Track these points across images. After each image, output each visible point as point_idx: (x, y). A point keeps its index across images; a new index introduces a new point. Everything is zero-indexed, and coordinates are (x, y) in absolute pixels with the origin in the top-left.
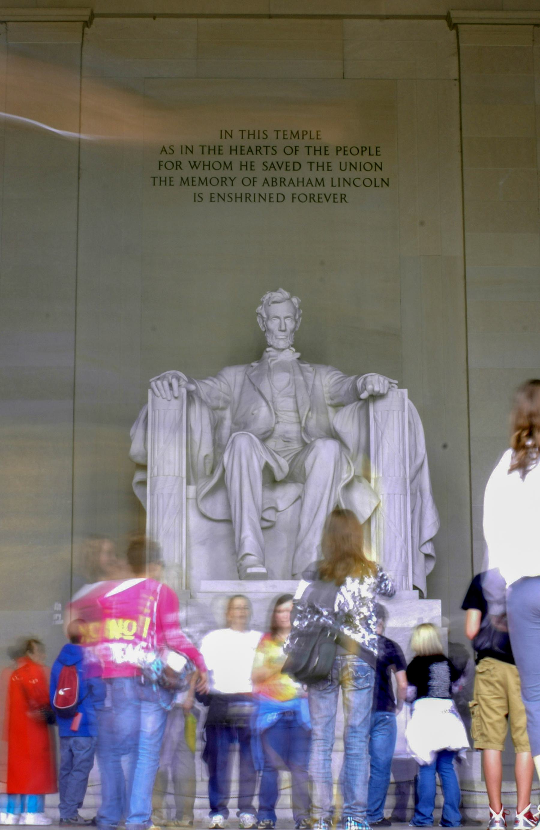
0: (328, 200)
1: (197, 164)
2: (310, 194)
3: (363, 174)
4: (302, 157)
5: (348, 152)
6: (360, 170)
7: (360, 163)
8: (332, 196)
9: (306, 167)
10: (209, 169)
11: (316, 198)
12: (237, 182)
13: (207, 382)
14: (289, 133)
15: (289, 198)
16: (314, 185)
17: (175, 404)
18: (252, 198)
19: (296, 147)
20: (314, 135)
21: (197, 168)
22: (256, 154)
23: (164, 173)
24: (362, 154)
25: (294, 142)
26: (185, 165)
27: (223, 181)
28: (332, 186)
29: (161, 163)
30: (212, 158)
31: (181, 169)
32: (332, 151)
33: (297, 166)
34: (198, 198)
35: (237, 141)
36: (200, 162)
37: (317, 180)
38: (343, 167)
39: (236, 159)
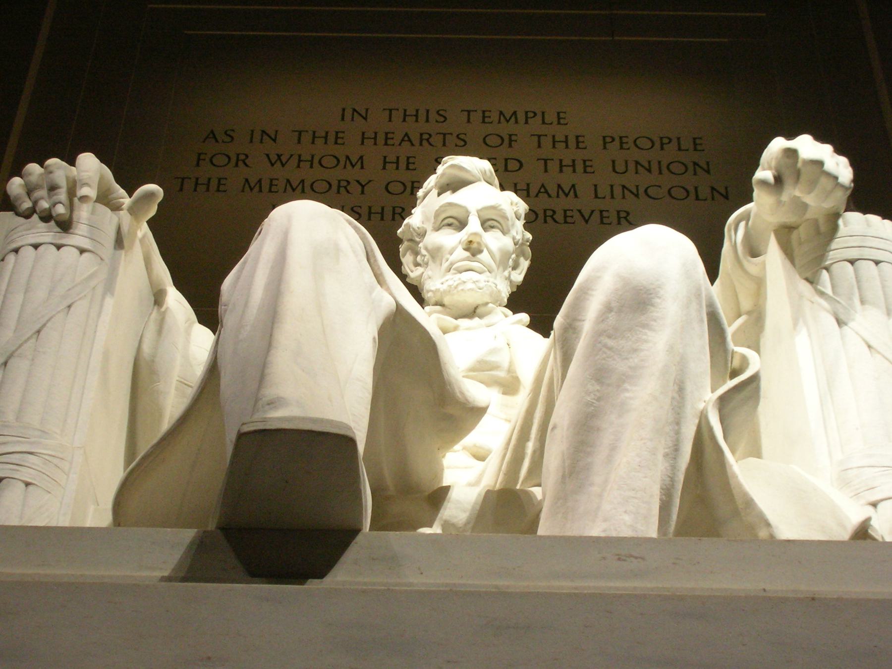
0: (587, 221)
1: (284, 159)
2: (545, 211)
5: (631, 144)
6: (660, 173)
7: (659, 162)
8: (596, 215)
10: (311, 167)
11: (559, 217)
14: (495, 116)
19: (510, 136)
20: (551, 117)
21: (283, 165)
22: (421, 144)
24: (662, 149)
25: (505, 129)
28: (596, 196)
29: (202, 157)
31: (247, 165)
36: (292, 156)
37: (559, 186)
38: (620, 168)
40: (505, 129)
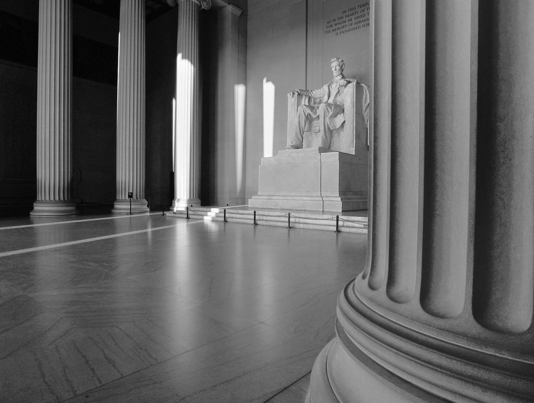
12: (347, 26)
15: (362, 26)
25: (363, 8)
26: (334, 26)
27: (343, 27)
34: (337, 34)
39: (347, 19)
40: (363, 8)
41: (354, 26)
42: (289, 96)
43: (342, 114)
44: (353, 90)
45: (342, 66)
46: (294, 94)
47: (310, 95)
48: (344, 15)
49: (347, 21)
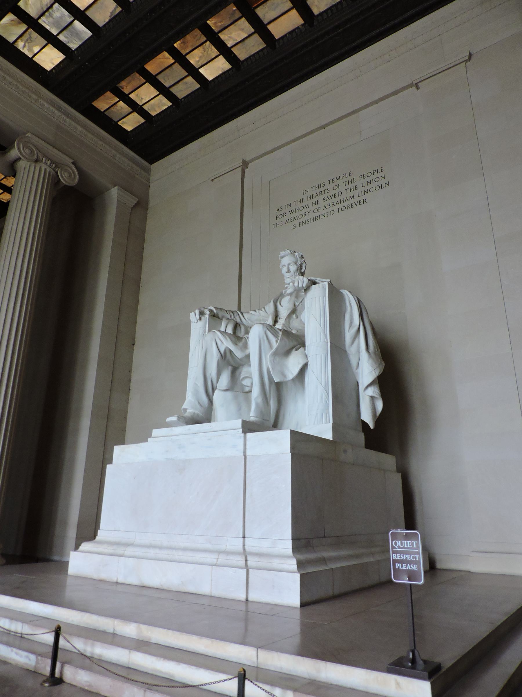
3: (375, 184)
4: (343, 188)
9: (344, 192)
11: (350, 207)
12: (311, 213)
13: (251, 312)
15: (336, 211)
16: (349, 199)
17: (201, 323)
18: (318, 218)
23: (279, 220)
25: (337, 183)
26: (288, 214)
27: (305, 215)
30: (300, 205)
32: (357, 179)
33: (340, 194)
35: (311, 193)
39: (310, 202)
40: (337, 183)
41: (323, 212)
42: (194, 316)
43: (302, 349)
44: (324, 297)
45: (301, 266)
46: (202, 313)
47: (238, 320)
48: (305, 196)
49: (310, 205)
